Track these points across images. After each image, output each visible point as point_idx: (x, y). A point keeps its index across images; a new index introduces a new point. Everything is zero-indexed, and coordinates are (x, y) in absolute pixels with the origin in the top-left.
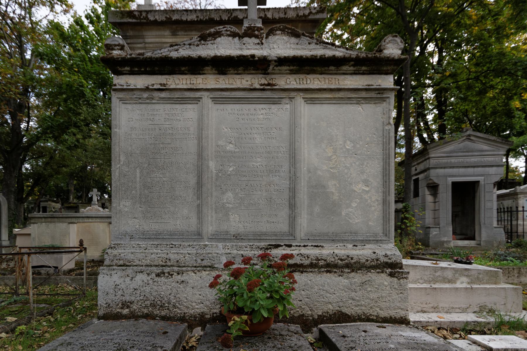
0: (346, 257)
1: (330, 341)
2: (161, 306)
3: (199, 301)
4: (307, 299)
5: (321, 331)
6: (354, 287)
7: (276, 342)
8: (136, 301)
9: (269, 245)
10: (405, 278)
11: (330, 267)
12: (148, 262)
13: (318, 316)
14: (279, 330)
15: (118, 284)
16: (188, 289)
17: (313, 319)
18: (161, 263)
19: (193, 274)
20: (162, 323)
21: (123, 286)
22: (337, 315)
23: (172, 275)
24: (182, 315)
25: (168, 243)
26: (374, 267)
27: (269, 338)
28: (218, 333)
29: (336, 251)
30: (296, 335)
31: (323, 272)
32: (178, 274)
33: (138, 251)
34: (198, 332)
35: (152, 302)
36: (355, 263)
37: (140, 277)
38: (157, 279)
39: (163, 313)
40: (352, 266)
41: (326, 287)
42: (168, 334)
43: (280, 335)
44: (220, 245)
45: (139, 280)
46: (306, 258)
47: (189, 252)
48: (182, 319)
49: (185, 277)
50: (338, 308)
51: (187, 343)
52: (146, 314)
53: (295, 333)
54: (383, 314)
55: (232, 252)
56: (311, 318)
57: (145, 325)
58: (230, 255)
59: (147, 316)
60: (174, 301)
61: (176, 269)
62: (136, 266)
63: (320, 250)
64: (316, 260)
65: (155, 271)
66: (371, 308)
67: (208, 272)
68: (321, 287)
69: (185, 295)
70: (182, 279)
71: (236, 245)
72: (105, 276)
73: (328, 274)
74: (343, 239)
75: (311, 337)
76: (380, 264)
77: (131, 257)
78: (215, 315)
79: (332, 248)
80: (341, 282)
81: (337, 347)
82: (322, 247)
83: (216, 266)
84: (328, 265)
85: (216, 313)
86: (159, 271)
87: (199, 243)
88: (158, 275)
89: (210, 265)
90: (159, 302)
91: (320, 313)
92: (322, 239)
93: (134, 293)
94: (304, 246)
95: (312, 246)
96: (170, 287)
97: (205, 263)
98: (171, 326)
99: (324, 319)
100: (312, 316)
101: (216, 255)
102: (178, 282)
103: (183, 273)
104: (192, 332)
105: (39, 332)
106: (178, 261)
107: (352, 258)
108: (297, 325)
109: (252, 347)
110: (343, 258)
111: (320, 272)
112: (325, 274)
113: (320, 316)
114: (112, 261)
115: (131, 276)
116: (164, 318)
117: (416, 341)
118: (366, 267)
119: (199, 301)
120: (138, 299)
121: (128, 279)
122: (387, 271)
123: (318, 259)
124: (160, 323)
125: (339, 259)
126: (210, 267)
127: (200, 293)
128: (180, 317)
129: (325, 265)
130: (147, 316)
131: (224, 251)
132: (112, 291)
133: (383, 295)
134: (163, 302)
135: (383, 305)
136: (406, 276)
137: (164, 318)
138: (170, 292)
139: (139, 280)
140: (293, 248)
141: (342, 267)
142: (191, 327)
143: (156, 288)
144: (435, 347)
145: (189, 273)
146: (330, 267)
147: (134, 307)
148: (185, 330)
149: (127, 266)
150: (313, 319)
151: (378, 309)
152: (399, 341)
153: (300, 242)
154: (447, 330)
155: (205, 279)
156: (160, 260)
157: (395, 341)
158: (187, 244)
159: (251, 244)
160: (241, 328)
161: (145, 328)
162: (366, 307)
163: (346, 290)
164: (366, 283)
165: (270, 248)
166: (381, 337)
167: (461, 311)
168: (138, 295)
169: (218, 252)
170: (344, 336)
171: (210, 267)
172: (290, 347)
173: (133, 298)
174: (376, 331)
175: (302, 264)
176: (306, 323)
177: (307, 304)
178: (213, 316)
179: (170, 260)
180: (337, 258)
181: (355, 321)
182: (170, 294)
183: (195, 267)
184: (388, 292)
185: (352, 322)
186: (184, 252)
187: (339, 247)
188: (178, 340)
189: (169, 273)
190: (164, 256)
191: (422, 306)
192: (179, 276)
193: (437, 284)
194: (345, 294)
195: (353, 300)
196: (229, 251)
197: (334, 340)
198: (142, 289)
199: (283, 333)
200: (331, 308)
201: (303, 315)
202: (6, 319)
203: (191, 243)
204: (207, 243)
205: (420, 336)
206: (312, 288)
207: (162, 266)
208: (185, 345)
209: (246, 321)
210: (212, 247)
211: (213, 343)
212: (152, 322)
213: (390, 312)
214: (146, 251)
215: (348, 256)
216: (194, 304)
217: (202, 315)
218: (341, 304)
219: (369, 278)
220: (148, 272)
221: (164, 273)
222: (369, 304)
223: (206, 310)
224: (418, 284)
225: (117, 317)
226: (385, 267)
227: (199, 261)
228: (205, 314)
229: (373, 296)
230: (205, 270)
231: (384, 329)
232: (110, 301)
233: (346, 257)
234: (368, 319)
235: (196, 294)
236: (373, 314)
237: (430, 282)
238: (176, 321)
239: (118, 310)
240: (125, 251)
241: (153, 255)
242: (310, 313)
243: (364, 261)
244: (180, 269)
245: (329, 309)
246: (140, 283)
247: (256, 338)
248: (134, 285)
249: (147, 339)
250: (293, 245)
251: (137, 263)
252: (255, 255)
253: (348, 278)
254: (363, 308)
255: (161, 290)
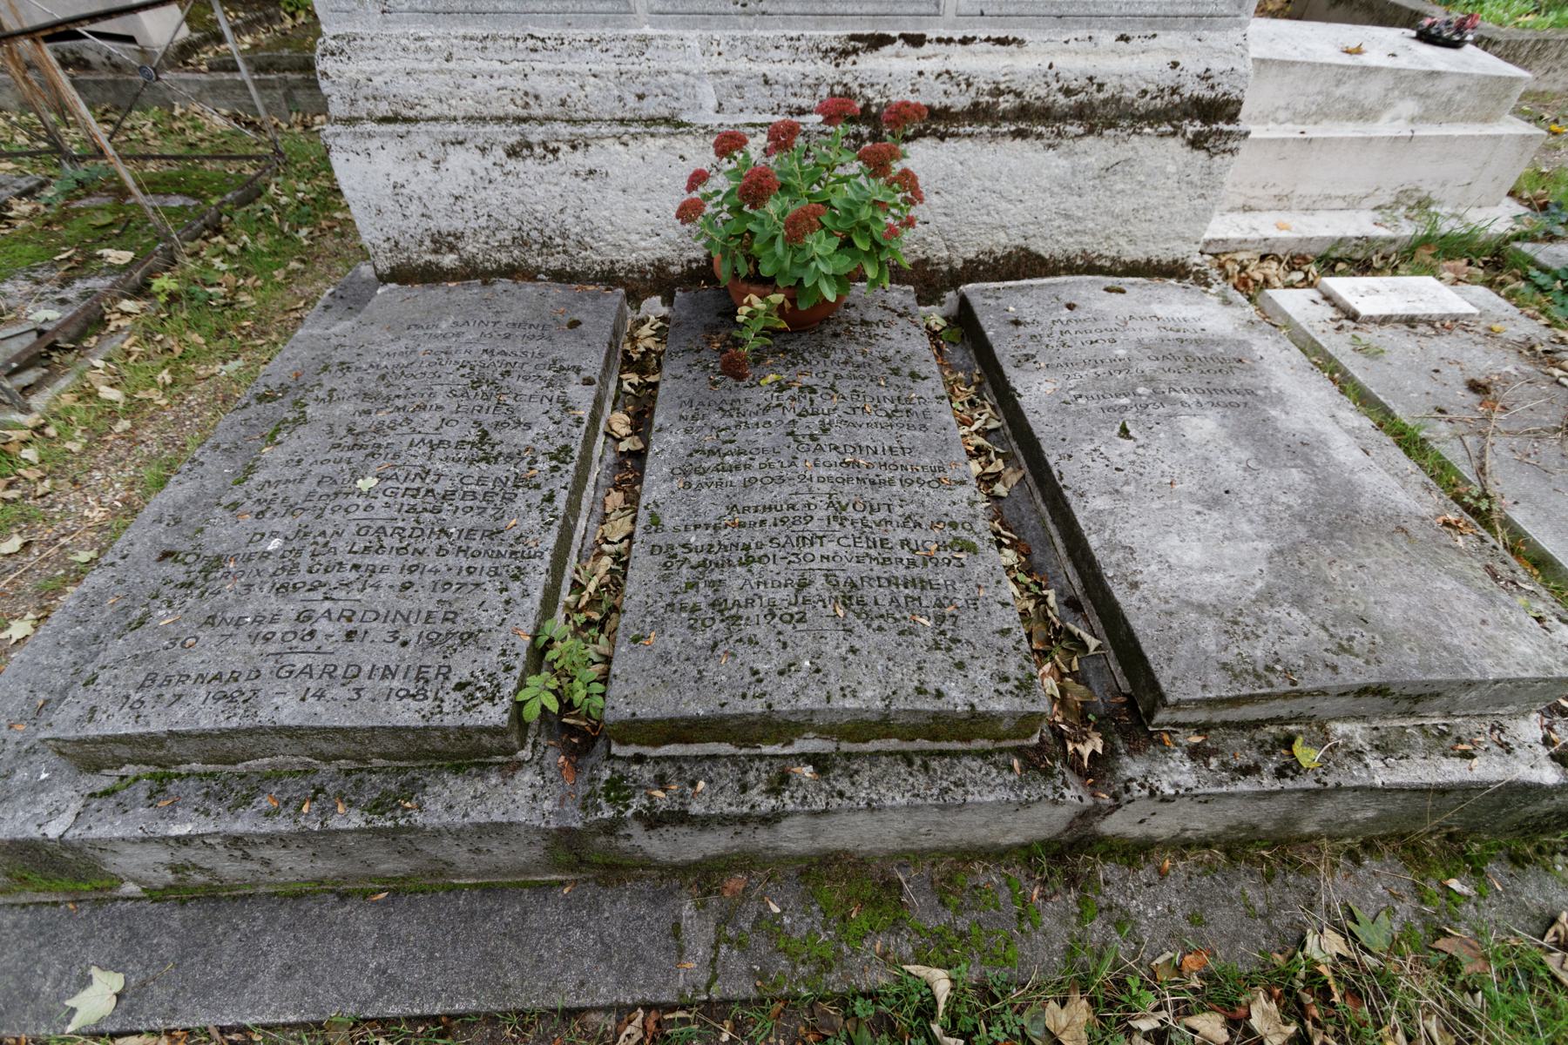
0: (1083, 81)
1: (982, 334)
2: (544, 245)
3: (648, 229)
4: (945, 219)
5: (964, 302)
6: (1080, 180)
7: (852, 347)
8: (468, 233)
9: (853, 38)
10: (1231, 151)
11: (1029, 117)
12: (470, 107)
13: (965, 261)
14: (862, 308)
15: (400, 181)
16: (612, 194)
17: (951, 269)
18: (511, 109)
19: (621, 148)
20: (556, 291)
21: (415, 187)
22: (1015, 259)
23: (555, 151)
24: (606, 268)
25: (519, 33)
26: (1154, 117)
27: (836, 335)
28: (707, 320)
29: (1060, 62)
30: (901, 322)
31: (1003, 135)
32: (574, 147)
33: (425, 66)
34: (654, 306)
35: (517, 234)
36: (1105, 102)
37: (461, 161)
38: (511, 164)
39: (555, 263)
40: (1096, 113)
41: (1004, 184)
42: (583, 327)
43: (864, 323)
44: (693, 37)
45: (459, 170)
46: (963, 86)
47: (596, 68)
48: (609, 278)
49: (593, 158)
50: (1020, 242)
51: (633, 340)
52: (507, 265)
53: (900, 316)
54: (1132, 253)
55: (732, 66)
56: (945, 268)
57: (517, 299)
58: (726, 79)
59: (513, 272)
60: (578, 229)
61: (564, 130)
62: (436, 119)
63: (1011, 55)
64: (991, 94)
65: (501, 138)
66: (1108, 238)
67: (662, 142)
68: (988, 184)
69: (606, 213)
70: (590, 163)
71: (744, 40)
72: (352, 156)
73: (1018, 140)
74: (1093, 10)
75: (936, 316)
76: (1176, 106)
77: (408, 88)
78: (694, 265)
79: (1051, 46)
80: (1048, 167)
81: (994, 355)
82: (1020, 42)
83: (685, 118)
84: (1025, 112)
85: (696, 260)
86: (514, 139)
87: (623, 32)
88: (512, 153)
89: (666, 114)
90: (534, 234)
91: (971, 255)
92: (1026, 11)
93: (457, 208)
94: (965, 41)
95: (988, 39)
96: (558, 189)
97: (651, 108)
98: (581, 298)
99: (977, 270)
100: (949, 261)
101: (682, 77)
102: (577, 175)
103: (587, 145)
104: (638, 308)
105: (221, 290)
106: (563, 103)
107: (1100, 87)
108: (907, 287)
109: (794, 365)
110: (1074, 85)
111: (994, 136)
112: (1008, 142)
113: (971, 261)
114: (353, 102)
115: (431, 156)
116: (558, 276)
117: (1180, 335)
118: (1133, 116)
119: (648, 229)
120: (473, 224)
121: (425, 167)
122: (1190, 129)
123: (997, 92)
124: (552, 292)
125: (1060, 90)
126: (667, 121)
127: (646, 205)
128: (603, 271)
129: (1013, 111)
130: (513, 272)
131: (707, 64)
132: (388, 204)
133: (1152, 201)
134: (547, 232)
135: (1139, 229)
136: (1235, 145)
137: (558, 276)
138: (559, 204)
139: (459, 170)
140: (927, 49)
141: (1063, 118)
142: (634, 297)
143: (515, 192)
144: (1220, 349)
145: (606, 142)
146: (1029, 117)
147: (470, 248)
148: (621, 308)
149: (407, 120)
150: (951, 269)
151: (1123, 242)
152: (1144, 334)
153: (954, 26)
154: (1280, 262)
155: (657, 163)
156: (507, 100)
157: (1133, 336)
158: (582, 34)
159: (794, 34)
160: (770, 324)
161: (519, 312)
162: (1094, 235)
163: (1056, 189)
164: (1118, 168)
165: (855, 51)
166: (1102, 325)
167: (1344, 205)
168: (470, 214)
169: (686, 66)
170: (1017, 323)
171: (667, 121)
172: (885, 360)
173: (458, 225)
174: (1098, 305)
175: (947, 109)
176: (929, 281)
177: (941, 232)
178: (690, 268)
179: (537, 97)
180: (1055, 86)
181: (1055, 272)
182: (562, 211)
183: (622, 121)
184: (1166, 194)
185: (1046, 275)
186: (576, 68)
187: (1072, 42)
188: (610, 345)
189: (544, 144)
190: (515, 82)
191: (1250, 193)
192: (579, 154)
193: (1326, 123)
194: (1050, 200)
195: (1067, 217)
196: (721, 64)
197: (990, 334)
198: (477, 197)
199: (872, 315)
200: (1002, 242)
201: (926, 261)
202: (101, 257)
203: (595, 32)
204: (648, 30)
205: (1197, 314)
206: (962, 186)
207: (520, 120)
208: (628, 346)
209: (782, 305)
210: (665, 47)
211: (698, 351)
212: (529, 288)
213: (1152, 247)
214: (451, 65)
215: (1091, 79)
216: (634, 237)
217: (661, 266)
218: (1031, 230)
219: (1131, 154)
220: (480, 142)
221: (529, 146)
222: (1105, 228)
223: (668, 252)
224: (1271, 125)
225: (430, 275)
226: (1186, 115)
227: (632, 101)
228: (669, 264)
229: (1123, 205)
230: (652, 135)
231: (1120, 297)
232: (394, 234)
233: (1083, 81)
234: (1091, 268)
235: (635, 209)
236: (1107, 253)
237: (1305, 117)
238: (594, 281)
239: (428, 257)
240: (383, 66)
241: (479, 80)
242: (945, 254)
243: (1134, 95)
244: (576, 130)
245: (998, 244)
246: (465, 177)
247: (805, 337)
248: (447, 186)
249: (534, 346)
250: (931, 35)
251: (435, 109)
252: (805, 76)
253: (1071, 153)
254: (1086, 239)
255: (534, 199)
